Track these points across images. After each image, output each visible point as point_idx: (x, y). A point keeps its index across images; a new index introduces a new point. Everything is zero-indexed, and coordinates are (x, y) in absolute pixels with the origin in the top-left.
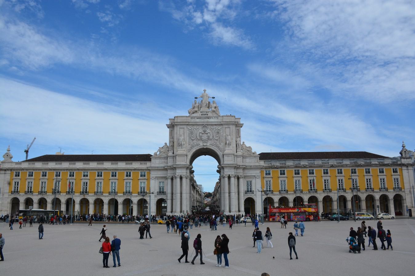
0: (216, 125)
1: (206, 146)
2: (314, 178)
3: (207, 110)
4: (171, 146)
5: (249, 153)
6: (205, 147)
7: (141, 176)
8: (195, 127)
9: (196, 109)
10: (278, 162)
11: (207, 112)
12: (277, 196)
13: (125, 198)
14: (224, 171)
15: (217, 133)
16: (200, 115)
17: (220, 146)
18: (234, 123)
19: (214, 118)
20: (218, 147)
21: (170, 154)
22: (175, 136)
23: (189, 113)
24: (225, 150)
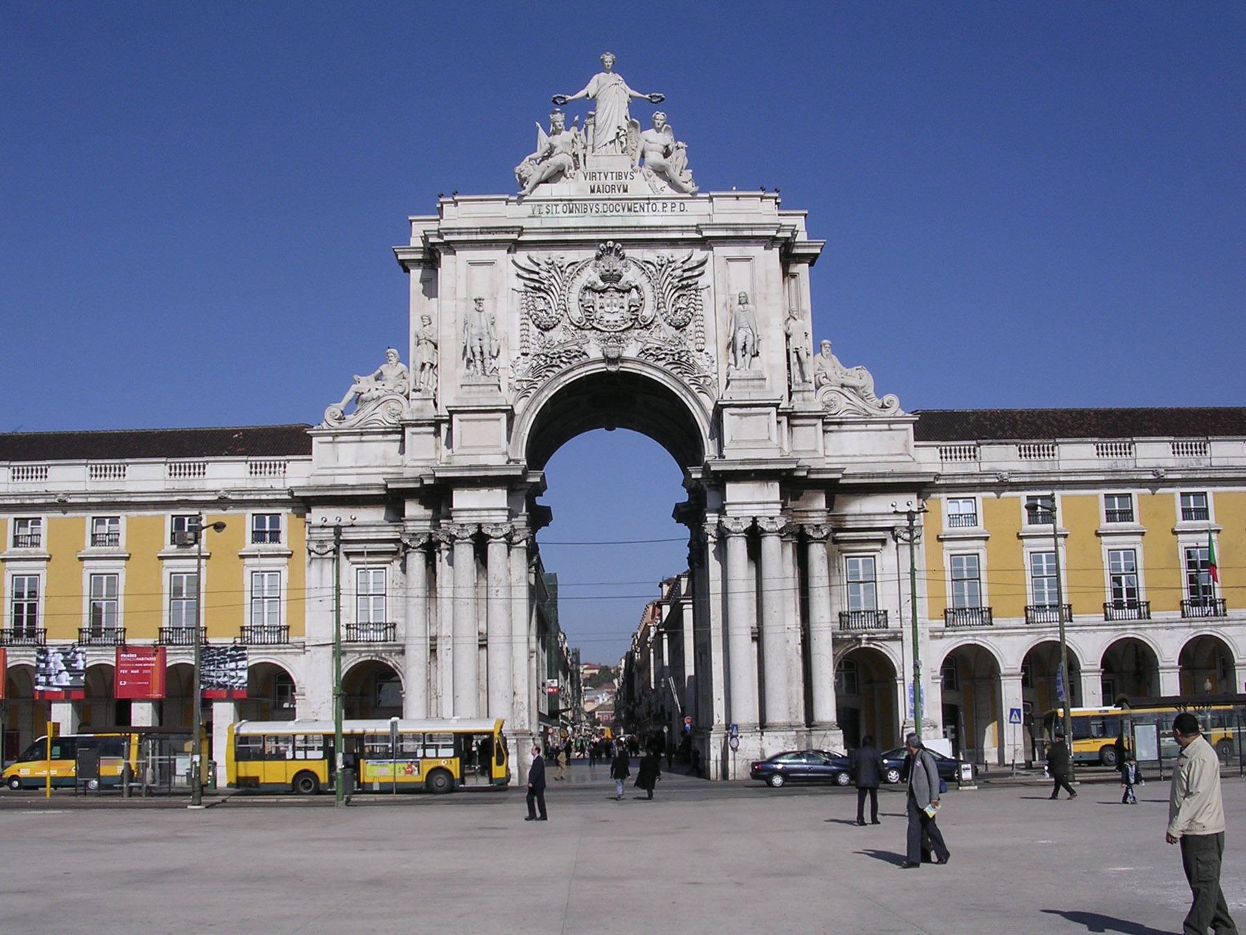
0: (673, 243)
1: (619, 359)
4: (423, 365)
5: (861, 404)
6: (613, 368)
7: (258, 536)
8: (556, 254)
10: (1013, 449)
11: (619, 175)
12: (1015, 638)
14: (724, 497)
15: (683, 288)
17: (699, 362)
18: (773, 233)
19: (660, 206)
20: (689, 367)
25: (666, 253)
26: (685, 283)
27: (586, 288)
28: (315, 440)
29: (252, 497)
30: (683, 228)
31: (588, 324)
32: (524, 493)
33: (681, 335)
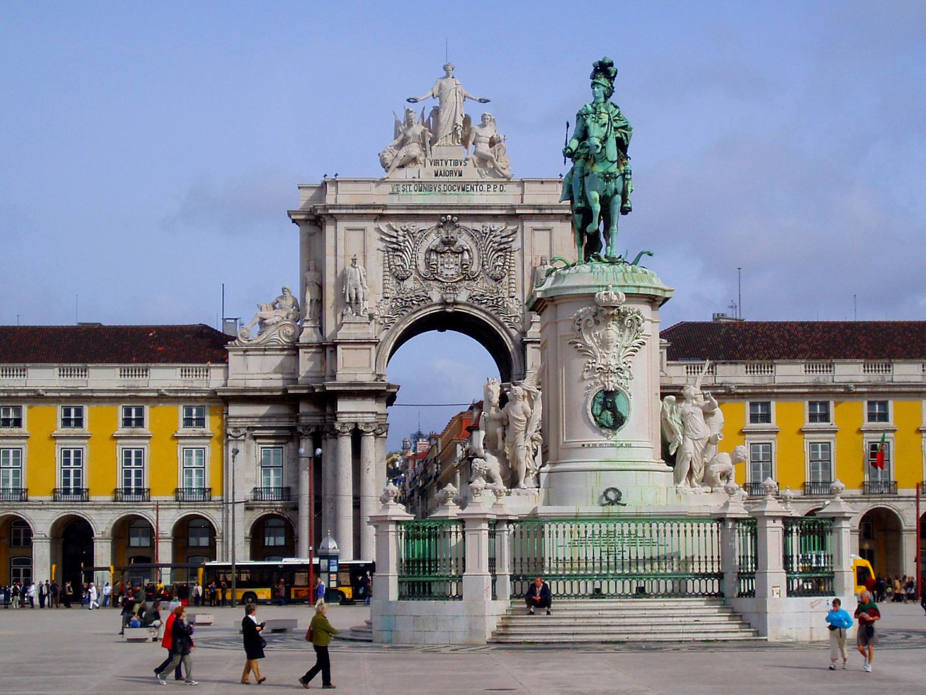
0: (495, 217)
1: (455, 303)
2: (886, 435)
3: (459, 153)
9: (414, 150)
10: (741, 368)
11: (456, 163)
13: (124, 513)
15: (501, 250)
16: (428, 174)
17: (511, 306)
19: (485, 186)
21: (309, 335)
22: (330, 260)
23: (386, 167)
24: (531, 323)
25: (489, 225)
26: (502, 246)
27: (432, 250)
28: (230, 354)
29: (184, 394)
30: (502, 207)
31: (432, 275)
32: (385, 398)
33: (499, 286)
